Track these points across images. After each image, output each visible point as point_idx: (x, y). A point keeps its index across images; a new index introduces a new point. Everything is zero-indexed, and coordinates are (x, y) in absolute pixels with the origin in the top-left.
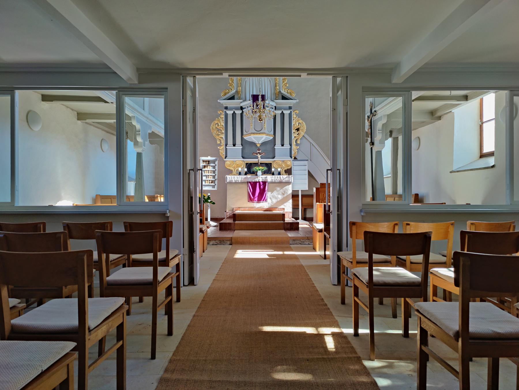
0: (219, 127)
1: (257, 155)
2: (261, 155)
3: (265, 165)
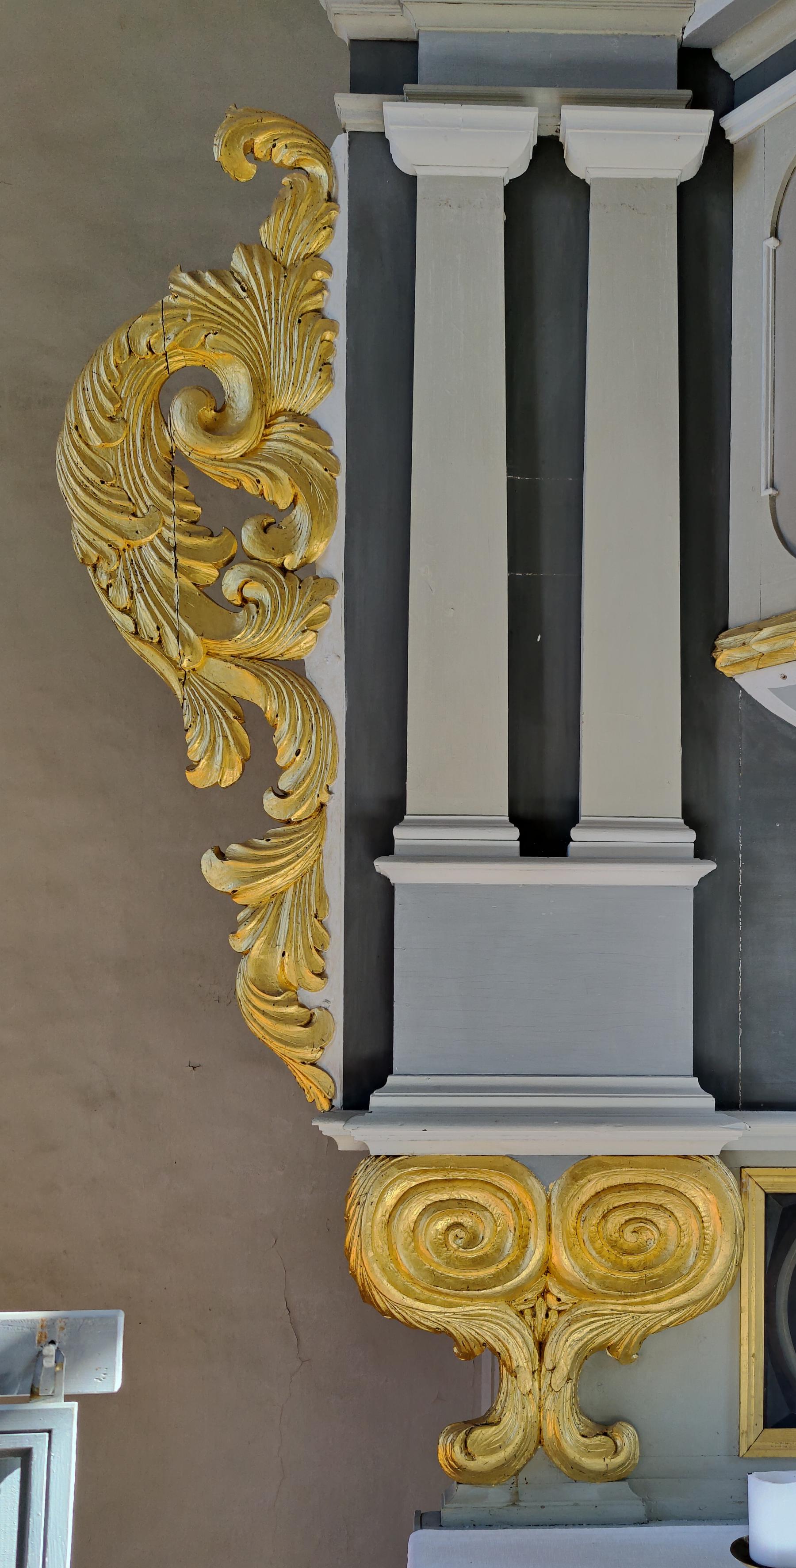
0: (238, 448)
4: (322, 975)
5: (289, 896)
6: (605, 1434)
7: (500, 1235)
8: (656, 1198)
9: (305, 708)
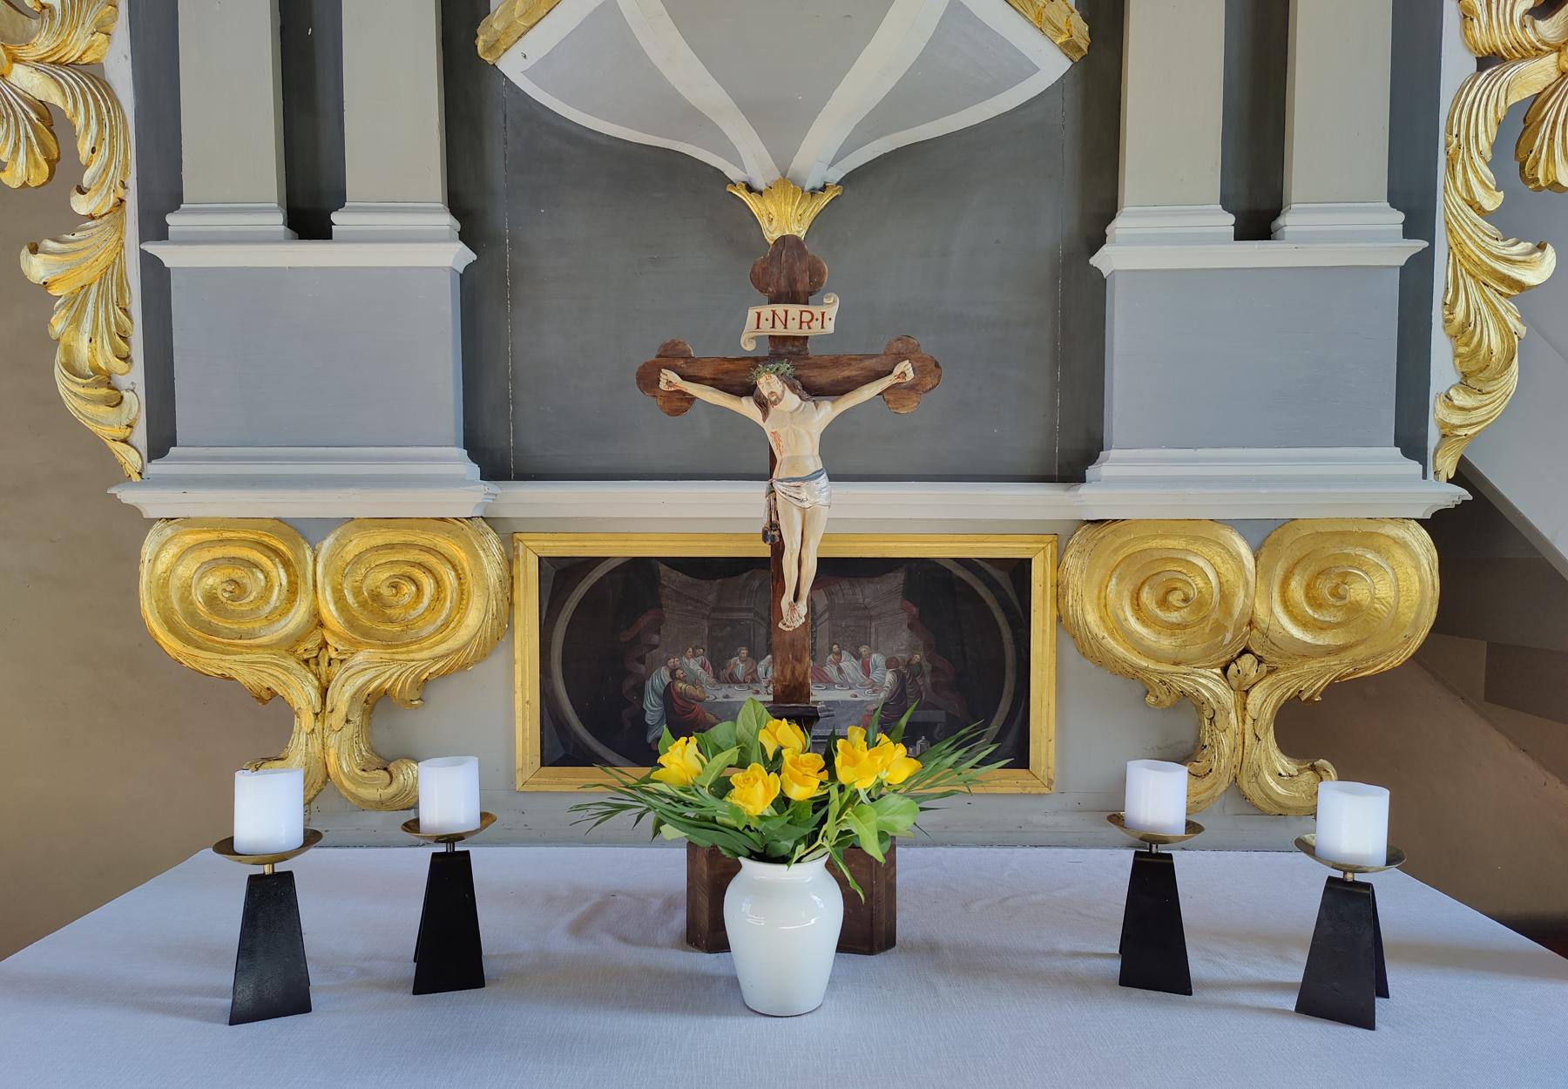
1: (746, 407)
2: (827, 411)
3: (909, 593)
4: (126, 359)
5: (94, 287)
6: (385, 769)
7: (268, 588)
8: (414, 556)
9: (98, 107)
